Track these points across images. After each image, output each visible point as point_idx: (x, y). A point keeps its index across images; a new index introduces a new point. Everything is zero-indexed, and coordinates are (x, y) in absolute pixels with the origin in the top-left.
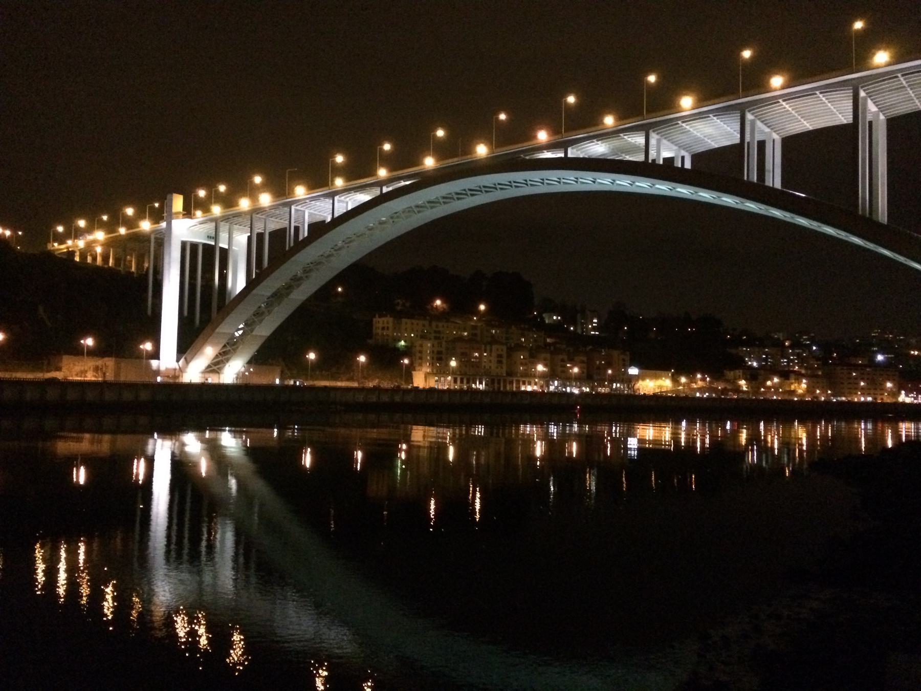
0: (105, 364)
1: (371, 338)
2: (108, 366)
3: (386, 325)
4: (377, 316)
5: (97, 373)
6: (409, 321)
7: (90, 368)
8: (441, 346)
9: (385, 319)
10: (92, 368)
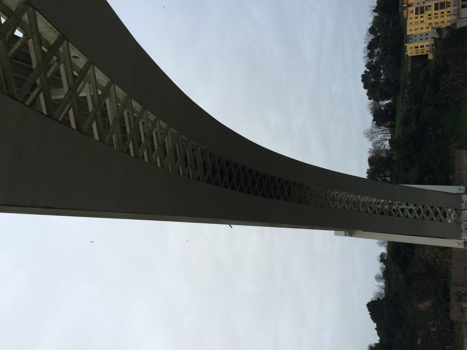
0: (456, 293)
1: (427, 55)
2: (458, 291)
3: (414, 49)
4: (406, 53)
5: (463, 300)
6: (409, 28)
7: (459, 304)
8: (430, 6)
9: (408, 50)
10: (460, 304)
